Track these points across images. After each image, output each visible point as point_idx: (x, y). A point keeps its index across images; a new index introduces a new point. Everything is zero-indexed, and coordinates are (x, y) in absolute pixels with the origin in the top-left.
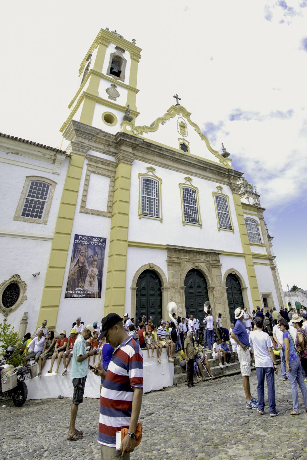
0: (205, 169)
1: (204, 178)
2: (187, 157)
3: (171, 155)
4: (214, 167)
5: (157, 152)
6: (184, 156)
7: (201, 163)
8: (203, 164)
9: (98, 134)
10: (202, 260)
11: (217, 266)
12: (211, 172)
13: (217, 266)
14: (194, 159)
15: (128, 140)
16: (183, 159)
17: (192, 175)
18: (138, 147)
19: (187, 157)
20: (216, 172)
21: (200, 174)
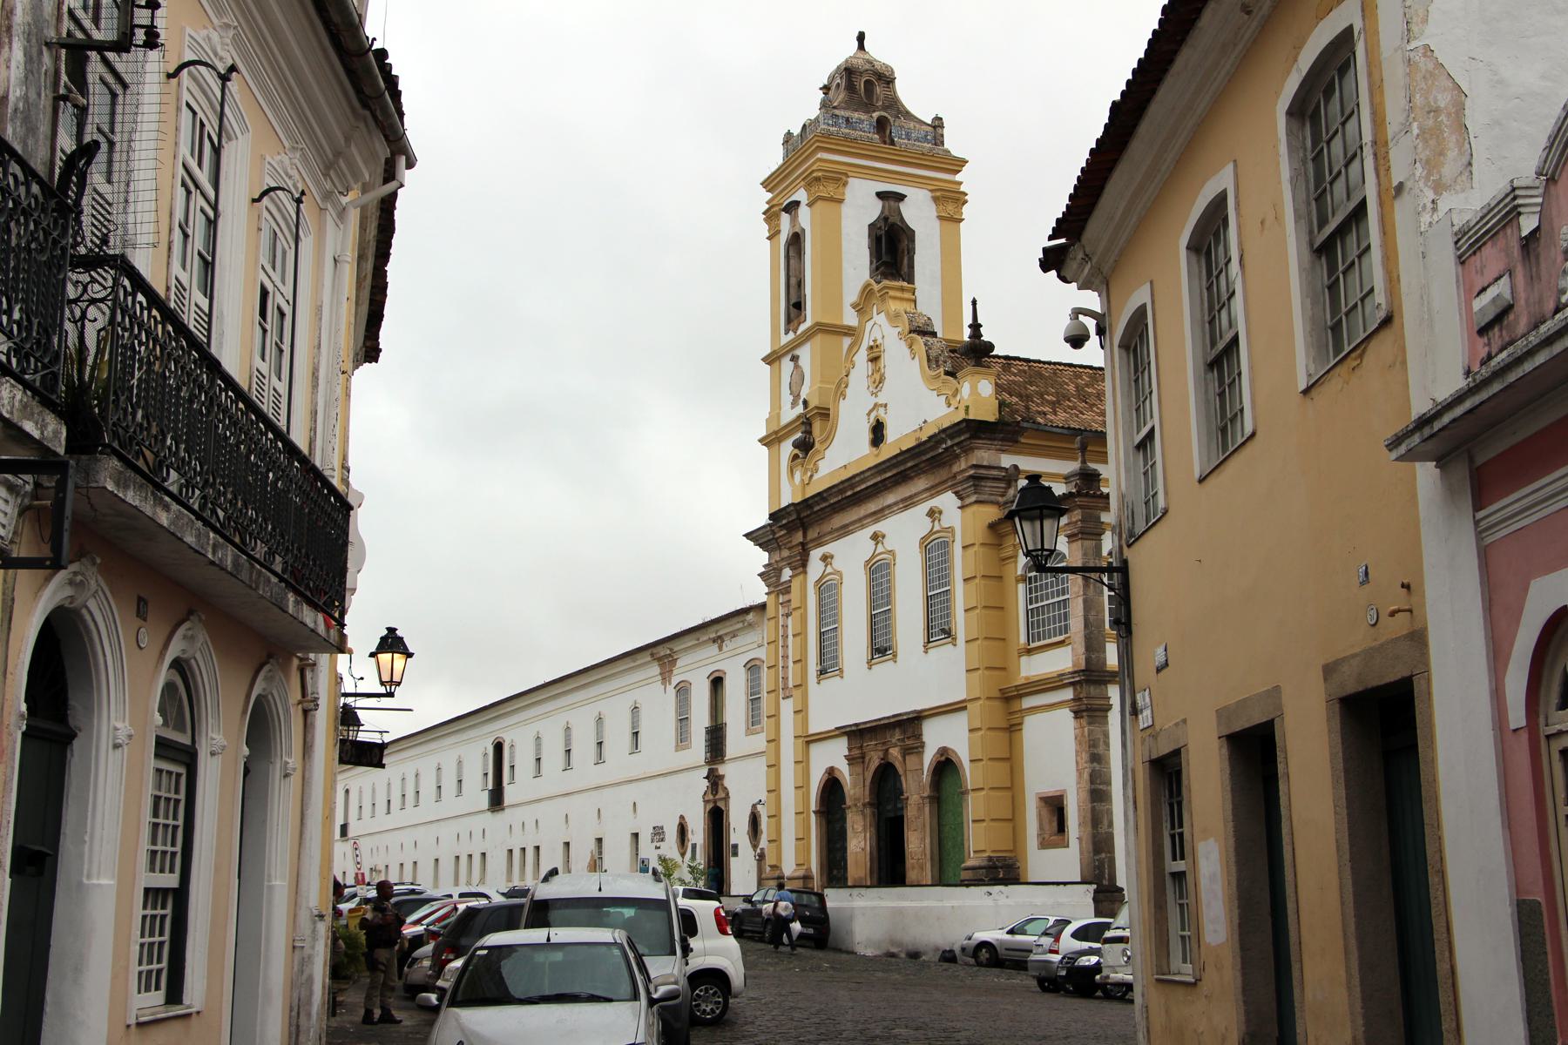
0: (902, 478)
1: (906, 508)
2: (857, 479)
3: (840, 498)
4: (913, 457)
5: (826, 507)
6: (854, 481)
7: (884, 471)
8: (890, 470)
9: (774, 533)
10: (894, 741)
11: (913, 748)
12: (919, 474)
13: (913, 748)
14: (869, 473)
15: (784, 522)
16: (859, 489)
17: (885, 517)
18: (805, 520)
19: (857, 479)
20: (923, 465)
21: (896, 504)
